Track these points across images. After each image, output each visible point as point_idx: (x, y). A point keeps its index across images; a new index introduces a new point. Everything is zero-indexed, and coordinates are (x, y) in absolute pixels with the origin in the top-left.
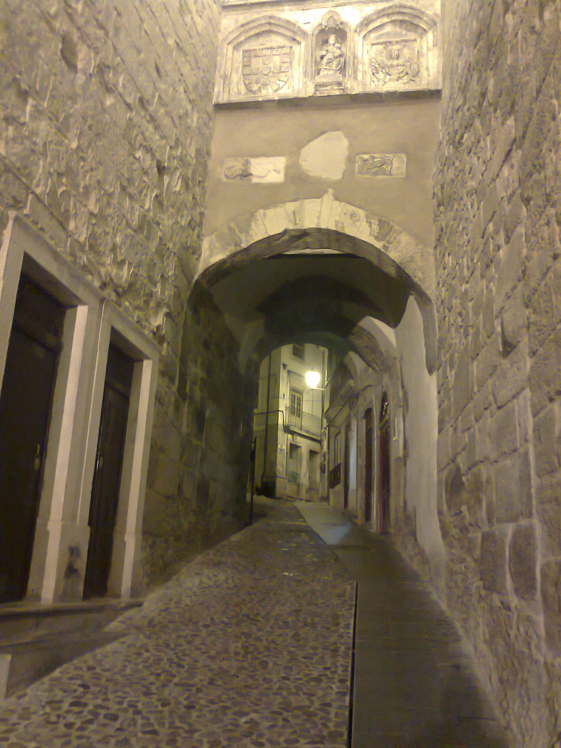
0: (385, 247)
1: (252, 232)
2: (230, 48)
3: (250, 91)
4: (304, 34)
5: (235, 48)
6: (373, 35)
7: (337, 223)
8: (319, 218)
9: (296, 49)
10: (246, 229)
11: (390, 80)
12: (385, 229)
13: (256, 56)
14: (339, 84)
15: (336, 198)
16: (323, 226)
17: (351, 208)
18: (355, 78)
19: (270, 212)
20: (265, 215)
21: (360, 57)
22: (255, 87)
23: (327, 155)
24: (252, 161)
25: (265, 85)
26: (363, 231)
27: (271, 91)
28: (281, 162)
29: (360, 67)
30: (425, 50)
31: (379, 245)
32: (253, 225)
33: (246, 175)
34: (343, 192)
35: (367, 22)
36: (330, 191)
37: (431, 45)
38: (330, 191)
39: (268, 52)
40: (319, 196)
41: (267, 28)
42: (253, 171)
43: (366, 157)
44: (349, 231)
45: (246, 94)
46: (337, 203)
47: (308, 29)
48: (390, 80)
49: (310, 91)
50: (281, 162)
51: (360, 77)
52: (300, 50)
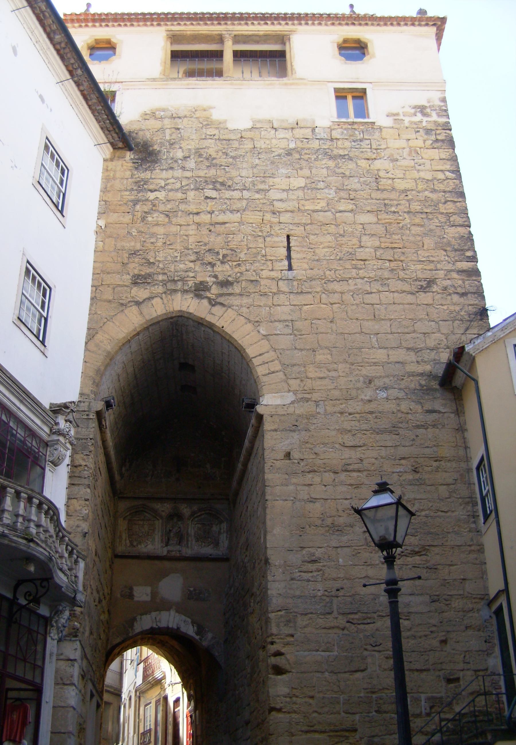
0: (200, 639)
1: (135, 628)
2: (122, 519)
3: (132, 545)
4: (161, 517)
5: (124, 519)
6: (196, 519)
7: (178, 624)
8: (168, 621)
9: (157, 522)
10: (132, 626)
11: (204, 546)
12: (200, 630)
13: (135, 524)
14: (180, 551)
15: (177, 611)
16: (170, 626)
17: (183, 617)
18: (188, 547)
19: (144, 617)
20: (141, 618)
21: (190, 532)
22: (135, 544)
23: (172, 587)
24: (135, 588)
25: (140, 543)
26: (190, 630)
27: (143, 546)
28: (148, 589)
29: (190, 539)
30: (222, 531)
31: (197, 637)
32: (135, 624)
33: (131, 596)
34: (180, 609)
35: (193, 513)
36: (174, 607)
37: (225, 530)
38: (174, 607)
39: (141, 523)
40: (168, 609)
41: (141, 509)
42: (135, 593)
43: (192, 589)
44: (183, 629)
45: (129, 547)
46: (177, 614)
47: (163, 514)
48: (204, 546)
49: (164, 552)
50: (148, 589)
51: (189, 544)
52: (158, 523)
